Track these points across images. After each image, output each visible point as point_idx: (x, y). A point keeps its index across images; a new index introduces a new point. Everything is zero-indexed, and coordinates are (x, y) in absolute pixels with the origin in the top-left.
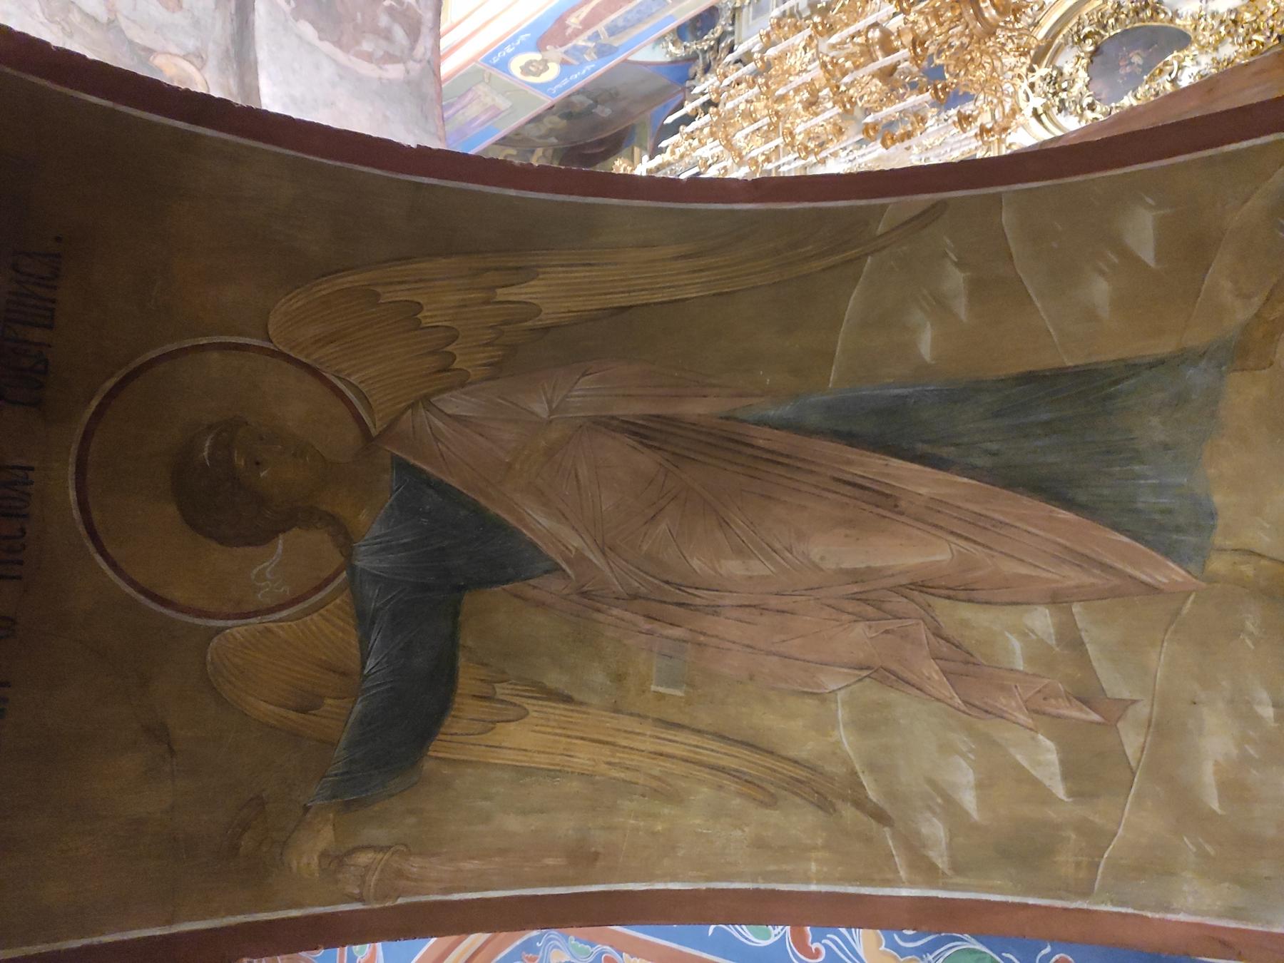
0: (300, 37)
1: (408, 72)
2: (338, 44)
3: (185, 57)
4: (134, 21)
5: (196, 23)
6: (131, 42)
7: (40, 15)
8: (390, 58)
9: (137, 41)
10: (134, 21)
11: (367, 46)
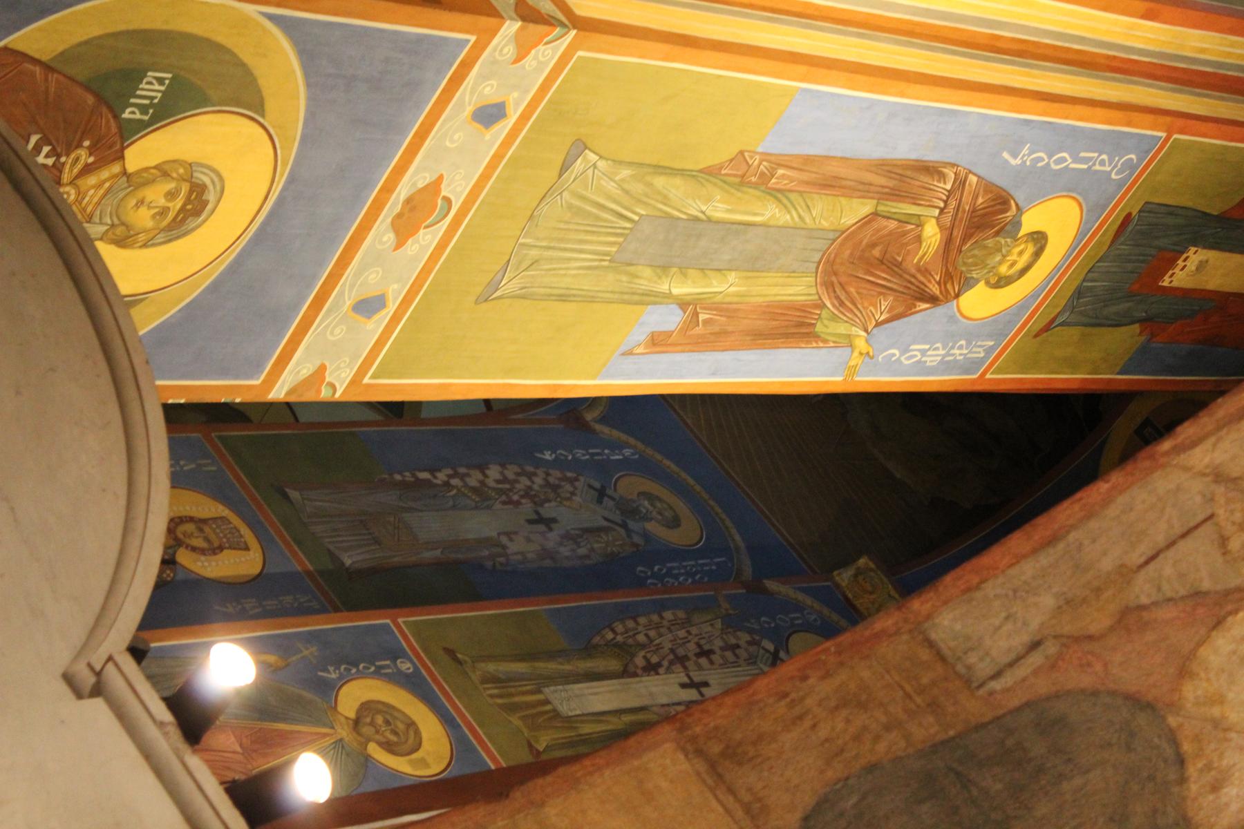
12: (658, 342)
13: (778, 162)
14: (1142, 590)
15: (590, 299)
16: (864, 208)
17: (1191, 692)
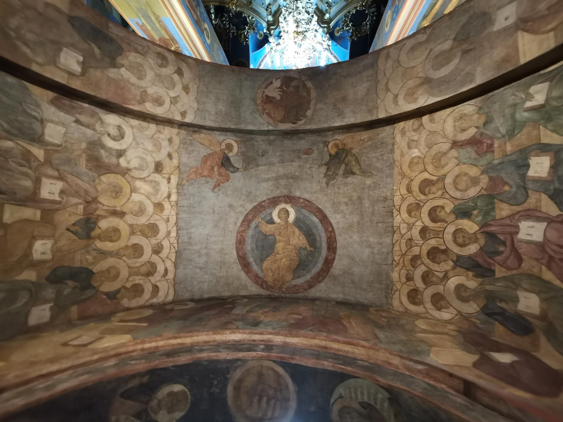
0: (313, 115)
1: (307, 80)
2: (309, 103)
3: (327, 146)
5: (313, 144)
6: (330, 160)
8: (305, 86)
10: (322, 160)
11: (305, 94)
12: (137, 23)
13: (162, 22)
14: (132, 44)
15: (132, 9)
16: (168, 38)
17: (127, 53)
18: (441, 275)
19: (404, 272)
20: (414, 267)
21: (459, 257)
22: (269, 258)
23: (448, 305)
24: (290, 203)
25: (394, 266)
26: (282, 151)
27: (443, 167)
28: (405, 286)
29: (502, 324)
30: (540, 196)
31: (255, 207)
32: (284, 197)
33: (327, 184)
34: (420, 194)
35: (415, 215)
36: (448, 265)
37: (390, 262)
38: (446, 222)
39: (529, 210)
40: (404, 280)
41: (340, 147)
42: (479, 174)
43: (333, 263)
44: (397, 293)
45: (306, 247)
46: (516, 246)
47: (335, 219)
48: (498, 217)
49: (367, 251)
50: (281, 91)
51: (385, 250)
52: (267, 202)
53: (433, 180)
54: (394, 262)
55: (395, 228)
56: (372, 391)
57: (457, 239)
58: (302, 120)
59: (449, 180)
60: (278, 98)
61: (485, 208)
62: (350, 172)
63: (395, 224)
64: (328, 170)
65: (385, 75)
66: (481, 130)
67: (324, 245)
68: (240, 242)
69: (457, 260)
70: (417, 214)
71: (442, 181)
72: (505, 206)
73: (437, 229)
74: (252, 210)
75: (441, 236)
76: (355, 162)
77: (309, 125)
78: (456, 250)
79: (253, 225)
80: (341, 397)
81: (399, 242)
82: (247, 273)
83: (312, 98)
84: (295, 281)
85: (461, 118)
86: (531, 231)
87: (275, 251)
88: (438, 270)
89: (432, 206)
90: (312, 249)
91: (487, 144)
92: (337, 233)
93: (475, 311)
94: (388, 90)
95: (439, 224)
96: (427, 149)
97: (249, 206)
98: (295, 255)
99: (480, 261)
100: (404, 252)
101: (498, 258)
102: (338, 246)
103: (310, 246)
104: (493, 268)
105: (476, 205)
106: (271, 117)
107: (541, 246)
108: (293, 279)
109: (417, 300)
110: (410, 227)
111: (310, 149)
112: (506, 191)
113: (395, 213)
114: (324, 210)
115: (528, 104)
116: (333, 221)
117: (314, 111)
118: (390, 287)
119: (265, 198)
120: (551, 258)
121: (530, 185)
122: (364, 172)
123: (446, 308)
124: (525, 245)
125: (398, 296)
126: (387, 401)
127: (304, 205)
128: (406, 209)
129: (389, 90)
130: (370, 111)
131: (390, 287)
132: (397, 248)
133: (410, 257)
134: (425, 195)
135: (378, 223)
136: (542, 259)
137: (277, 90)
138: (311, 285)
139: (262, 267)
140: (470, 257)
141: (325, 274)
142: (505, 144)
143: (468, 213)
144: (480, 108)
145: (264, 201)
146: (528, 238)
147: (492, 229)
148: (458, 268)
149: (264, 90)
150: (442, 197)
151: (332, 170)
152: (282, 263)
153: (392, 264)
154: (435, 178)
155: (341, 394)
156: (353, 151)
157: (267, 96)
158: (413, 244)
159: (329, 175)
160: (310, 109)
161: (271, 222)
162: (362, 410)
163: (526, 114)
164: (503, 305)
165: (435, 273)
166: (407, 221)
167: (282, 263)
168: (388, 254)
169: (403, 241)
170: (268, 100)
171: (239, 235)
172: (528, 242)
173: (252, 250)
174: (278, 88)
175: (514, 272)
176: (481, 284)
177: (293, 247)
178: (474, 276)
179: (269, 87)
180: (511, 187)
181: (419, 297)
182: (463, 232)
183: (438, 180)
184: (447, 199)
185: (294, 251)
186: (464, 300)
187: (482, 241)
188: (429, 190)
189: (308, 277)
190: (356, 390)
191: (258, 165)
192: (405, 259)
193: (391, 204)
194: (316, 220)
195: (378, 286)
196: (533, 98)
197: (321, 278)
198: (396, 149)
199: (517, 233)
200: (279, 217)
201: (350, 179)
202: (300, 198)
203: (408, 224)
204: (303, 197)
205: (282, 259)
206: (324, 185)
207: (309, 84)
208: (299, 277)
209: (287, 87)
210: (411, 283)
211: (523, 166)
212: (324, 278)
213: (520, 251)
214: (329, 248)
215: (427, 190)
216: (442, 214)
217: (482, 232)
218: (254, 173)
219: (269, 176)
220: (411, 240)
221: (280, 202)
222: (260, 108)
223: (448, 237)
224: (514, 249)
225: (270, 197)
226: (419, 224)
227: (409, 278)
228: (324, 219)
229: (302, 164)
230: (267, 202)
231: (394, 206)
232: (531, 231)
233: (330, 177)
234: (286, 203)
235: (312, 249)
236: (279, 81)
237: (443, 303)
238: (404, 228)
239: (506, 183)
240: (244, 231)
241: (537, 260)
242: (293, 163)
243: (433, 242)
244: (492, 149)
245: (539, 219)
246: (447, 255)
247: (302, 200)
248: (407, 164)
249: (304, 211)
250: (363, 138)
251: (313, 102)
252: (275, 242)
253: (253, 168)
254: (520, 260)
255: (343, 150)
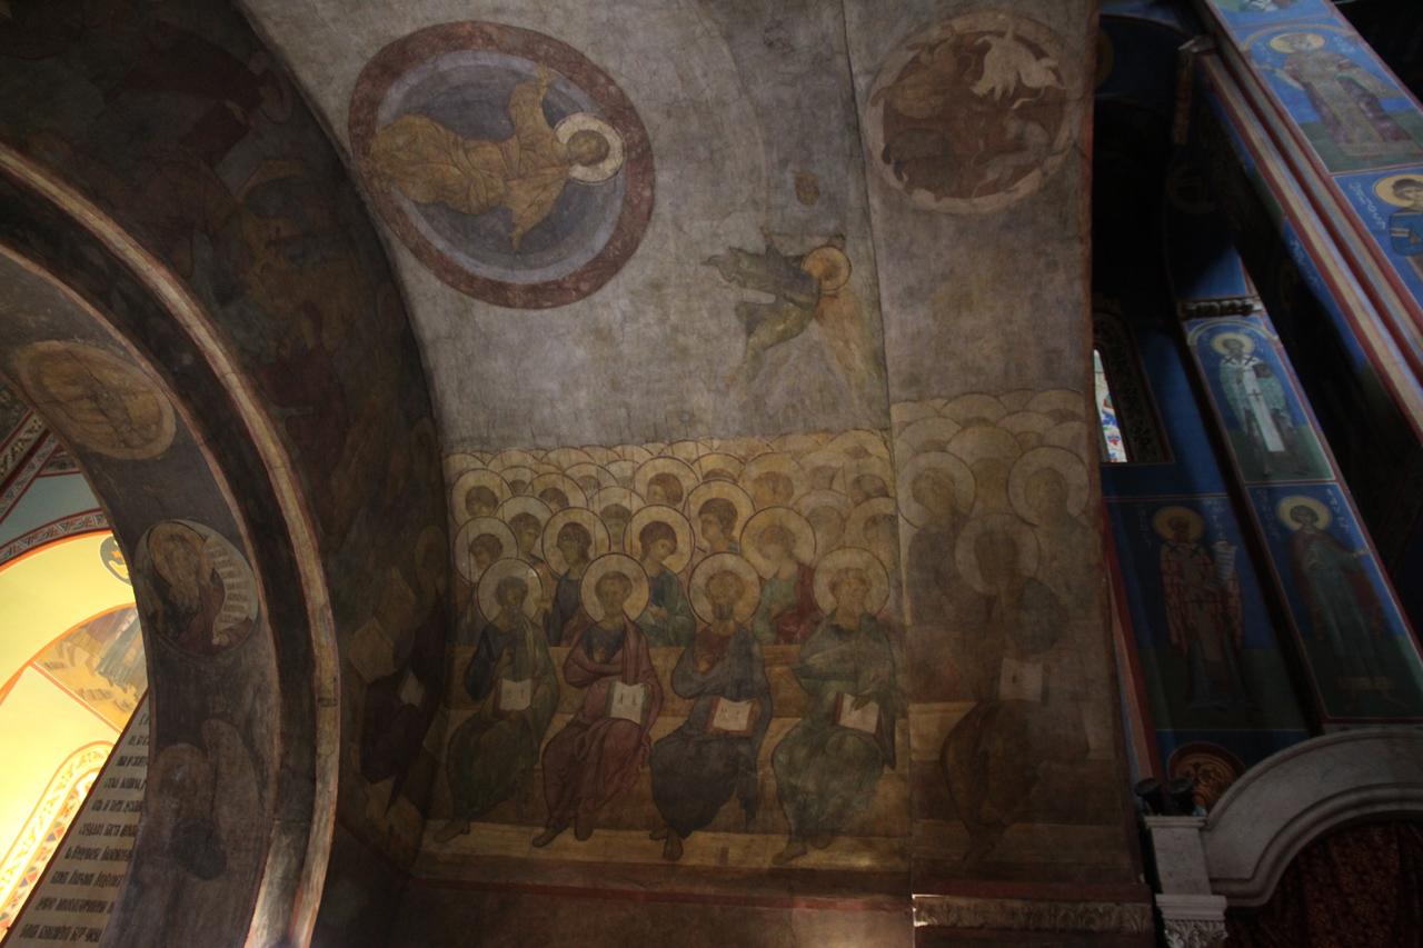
0: (916, 211)
1: (1045, 174)
2: (962, 193)
3: (828, 245)
4: (786, 234)
6: (786, 259)
7: (721, 280)
8: (1021, 172)
9: (791, 253)
11: (991, 176)
18: (537, 551)
19: (526, 476)
20: (541, 496)
21: (577, 584)
22: (440, 128)
23: (484, 566)
24: (630, 161)
25: (534, 452)
26: (798, 106)
27: (760, 550)
28: (498, 479)
29: (474, 657)
30: (682, 716)
31: (580, 59)
32: (644, 139)
33: (711, 261)
34: (701, 502)
35: (655, 493)
36: (556, 561)
37: (541, 442)
38: (643, 559)
39: (662, 699)
40: (510, 476)
41: (827, 284)
42: (737, 619)
43: (501, 305)
44: (479, 465)
45: (514, 226)
46: (602, 679)
47: (614, 301)
48: (652, 651)
49: (553, 386)
50: (1005, 92)
51: (564, 429)
52: (612, 89)
53: (732, 529)
54: (542, 453)
55: (619, 449)
56: (244, 592)
57: (609, 582)
58: (900, 178)
59: (730, 561)
60: (980, 89)
61: (670, 629)
62: (751, 319)
63: (628, 448)
64: (755, 256)
65: (1010, 414)
66: (824, 622)
67: (536, 277)
68: (449, 37)
69: (570, 581)
70: (658, 497)
71: (729, 548)
72: (673, 662)
73: (627, 542)
74: (567, 49)
75: (614, 549)
76: (784, 331)
77: (884, 202)
78: (590, 580)
79: (519, 63)
80: (204, 539)
81: (588, 459)
82: (366, 75)
83: (976, 201)
84: (415, 210)
85: (863, 581)
86: (627, 700)
87: (472, 143)
88: (546, 546)
89: (677, 530)
90: (515, 243)
91: (794, 634)
92: (578, 305)
93: (485, 613)
94: (966, 424)
95: (638, 544)
96: (806, 513)
97: (578, 41)
98: (482, 200)
99: (574, 622)
100: (568, 472)
101: (581, 652)
102: (546, 311)
103: (524, 237)
104: (564, 643)
105: (677, 614)
106: (900, 78)
107: (602, 712)
108: (417, 204)
109: (476, 507)
110: (628, 483)
111: (817, 192)
112: (698, 666)
113: (657, 447)
114: (632, 262)
115: (848, 701)
116: (609, 287)
117: (930, 213)
118: (485, 448)
119: (621, 82)
120: (587, 727)
121: (702, 703)
122: (756, 357)
123: (479, 563)
124: (604, 691)
125: (472, 466)
126: (244, 616)
127: (636, 202)
128: (666, 471)
129: (964, 428)
130: (913, 380)
131: (485, 448)
132: (574, 456)
133: (560, 486)
134: (700, 513)
135: (627, 406)
136: (584, 716)
137: (1011, 78)
138: (421, 252)
139: (409, 113)
140: (578, 604)
141: (462, 287)
142: (787, 663)
143: (663, 599)
144: (872, 618)
145: (611, 81)
146: (616, 696)
147: (632, 641)
148: (556, 583)
149: (1009, 36)
150: (695, 549)
151: (753, 270)
152: (444, 168)
153: (538, 449)
154: (736, 533)
155: (207, 537)
156: (814, 325)
157: (986, 48)
158: (589, 493)
159: (738, 261)
160: (938, 199)
161: (554, 117)
162: (208, 577)
163: (831, 696)
164: (505, 658)
165: (539, 540)
166: (637, 477)
167: (444, 168)
168: (559, 438)
169: (592, 470)
170: (970, 55)
171: (468, 27)
172: (609, 698)
173: (443, 77)
174: (1019, 80)
175: (561, 676)
176: (534, 625)
177: (502, 191)
178: (546, 611)
179: (1023, 49)
180: (704, 673)
181: (484, 509)
182: (625, 591)
183: (731, 540)
184: (691, 560)
185: (491, 195)
186: (500, 594)
187: (608, 626)
188: (710, 522)
189: (440, 244)
190: (230, 563)
191: (728, 37)
192: (554, 476)
193: (675, 435)
194: (601, 239)
195: (482, 418)
196: (857, 709)
197: (450, 279)
198: (814, 437)
199: (625, 681)
200: (574, 138)
201: (732, 321)
202: (652, 187)
203: (632, 479)
204: (659, 195)
205: (455, 166)
206: (708, 251)
207: (1026, 186)
208: (430, 219)
209: (1023, 113)
210: (508, 494)
211: (739, 692)
212: (452, 285)
213: (595, 685)
214: (533, 289)
215: (711, 517)
216: (659, 548)
217: (625, 626)
218: (699, 30)
219: (702, 82)
220: (598, 486)
221: (625, 130)
222: (935, 33)
223: (613, 564)
224: (599, 675)
225: (632, 97)
226: (634, 504)
227: (516, 487)
228: (605, 268)
229: (764, 174)
230: (612, 89)
231: (671, 444)
232: (627, 700)
233: (733, 264)
234: (626, 150)
235: (515, 243)
236: (1050, 80)
237: (485, 556)
238: (622, 470)
239: (712, 665)
240: (489, 40)
241: (583, 707)
242: (761, 148)
243: (599, 533)
244: (782, 642)
245: (646, 711)
246: (577, 562)
247: (647, 193)
248: (775, 469)
249: (618, 203)
250: (853, 346)
251: (961, 205)
252: (498, 139)
253: (716, 22)
254: (581, 685)
255: (819, 295)
